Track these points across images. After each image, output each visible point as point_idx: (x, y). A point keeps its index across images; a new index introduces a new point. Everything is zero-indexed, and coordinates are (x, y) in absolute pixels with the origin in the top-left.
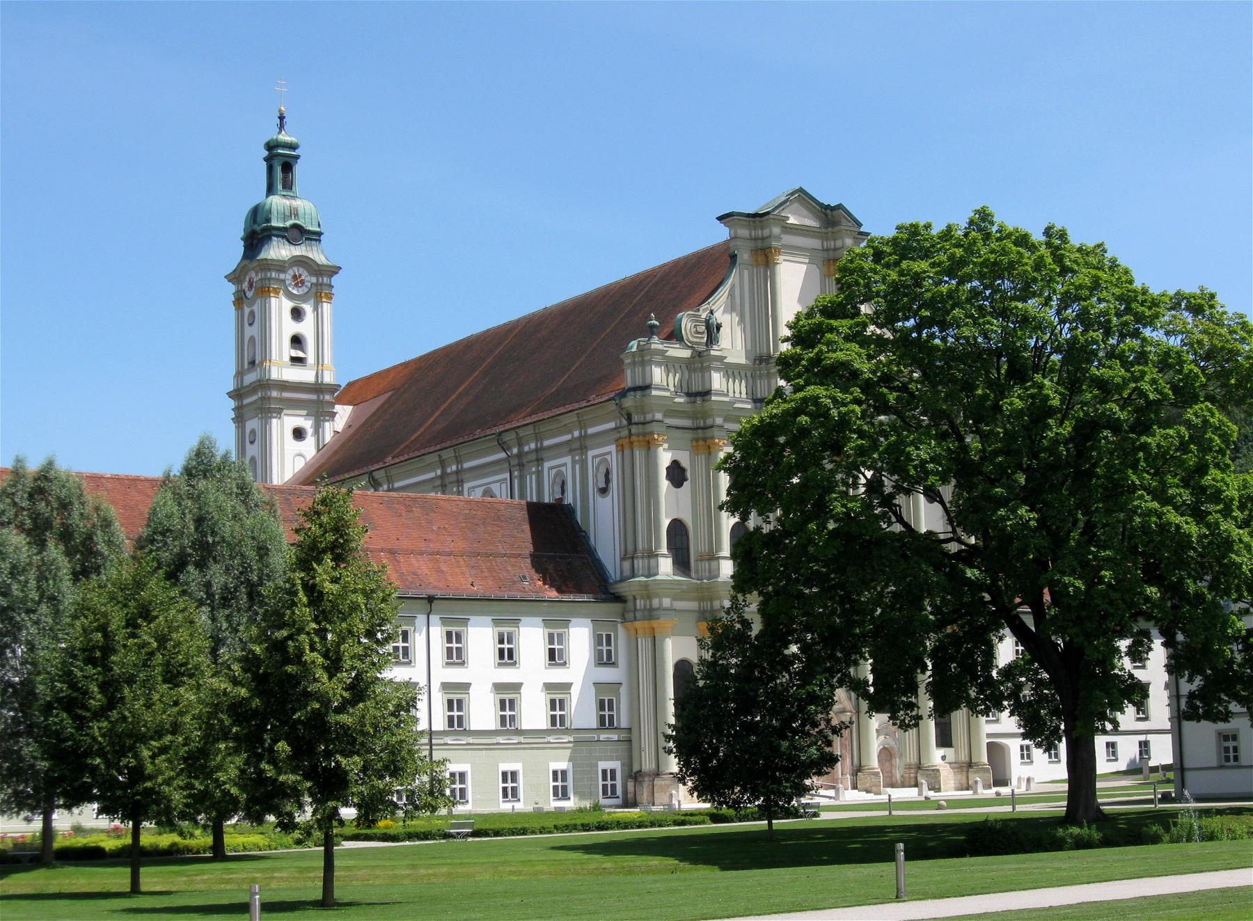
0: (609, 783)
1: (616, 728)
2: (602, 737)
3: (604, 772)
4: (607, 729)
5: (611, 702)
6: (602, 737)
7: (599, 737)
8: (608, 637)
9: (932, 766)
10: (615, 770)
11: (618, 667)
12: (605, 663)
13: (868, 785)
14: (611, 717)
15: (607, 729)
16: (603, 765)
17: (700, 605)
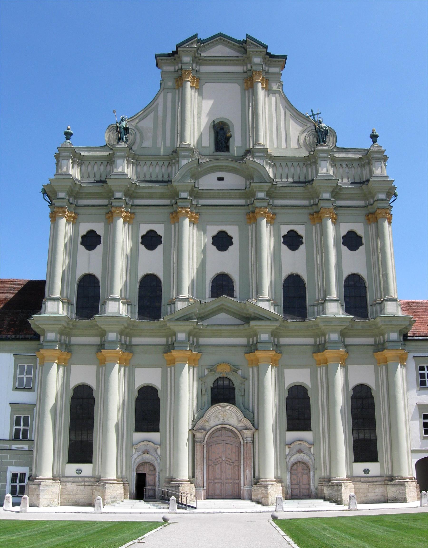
0: (18, 484)
1: (28, 440)
2: (14, 447)
3: (14, 476)
4: (21, 440)
5: (26, 419)
6: (14, 447)
7: (10, 446)
8: (29, 368)
9: (338, 480)
10: (25, 474)
11: (34, 391)
12: (24, 388)
13: (259, 496)
14: (25, 431)
15: (21, 440)
16: (12, 470)
17: (101, 339)
